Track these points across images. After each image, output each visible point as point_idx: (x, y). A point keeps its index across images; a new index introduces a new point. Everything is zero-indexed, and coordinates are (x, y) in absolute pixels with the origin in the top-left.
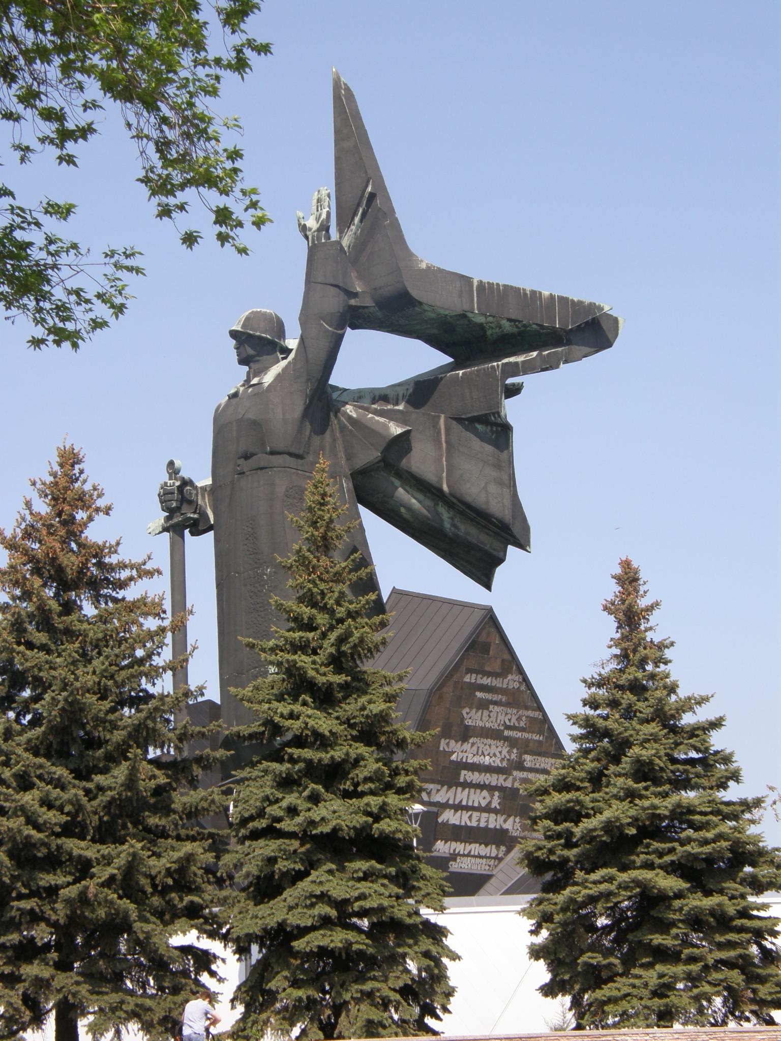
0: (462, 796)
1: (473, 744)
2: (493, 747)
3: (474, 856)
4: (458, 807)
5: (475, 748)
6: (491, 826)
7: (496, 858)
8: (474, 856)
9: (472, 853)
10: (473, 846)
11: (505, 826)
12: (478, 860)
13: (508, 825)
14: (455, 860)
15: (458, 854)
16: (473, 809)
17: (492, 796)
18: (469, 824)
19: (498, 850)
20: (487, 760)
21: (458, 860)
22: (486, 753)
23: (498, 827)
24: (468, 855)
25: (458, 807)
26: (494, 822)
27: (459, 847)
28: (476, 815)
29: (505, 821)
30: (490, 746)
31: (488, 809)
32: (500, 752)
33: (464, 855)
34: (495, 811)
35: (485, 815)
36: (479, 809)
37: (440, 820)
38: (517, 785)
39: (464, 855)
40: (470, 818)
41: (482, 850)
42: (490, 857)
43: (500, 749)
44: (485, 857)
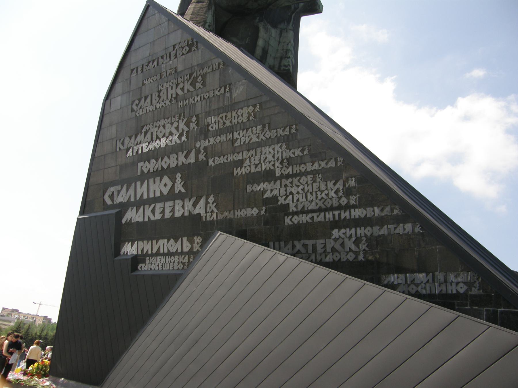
0: (142, 190)
1: (146, 133)
2: (168, 126)
3: (164, 254)
4: (140, 203)
5: (149, 135)
6: (178, 214)
7: (191, 252)
8: (164, 254)
9: (162, 251)
10: (161, 242)
11: (196, 211)
12: (169, 259)
13: (200, 209)
14: (144, 261)
15: (147, 255)
16: (155, 200)
17: (174, 182)
18: (152, 218)
19: (192, 242)
20: (163, 142)
21: (147, 262)
22: (160, 135)
23: (186, 214)
24: (158, 254)
25: (140, 203)
26: (181, 209)
27: (146, 246)
28: (159, 206)
29: (195, 205)
30: (164, 126)
31: (172, 196)
32: (177, 128)
33: (152, 255)
34: (181, 196)
35: (169, 204)
36: (163, 198)
37: (123, 221)
38: (201, 157)
39: (152, 255)
40: (153, 212)
41: (172, 246)
42: (182, 253)
43: (176, 124)
44: (176, 253)
